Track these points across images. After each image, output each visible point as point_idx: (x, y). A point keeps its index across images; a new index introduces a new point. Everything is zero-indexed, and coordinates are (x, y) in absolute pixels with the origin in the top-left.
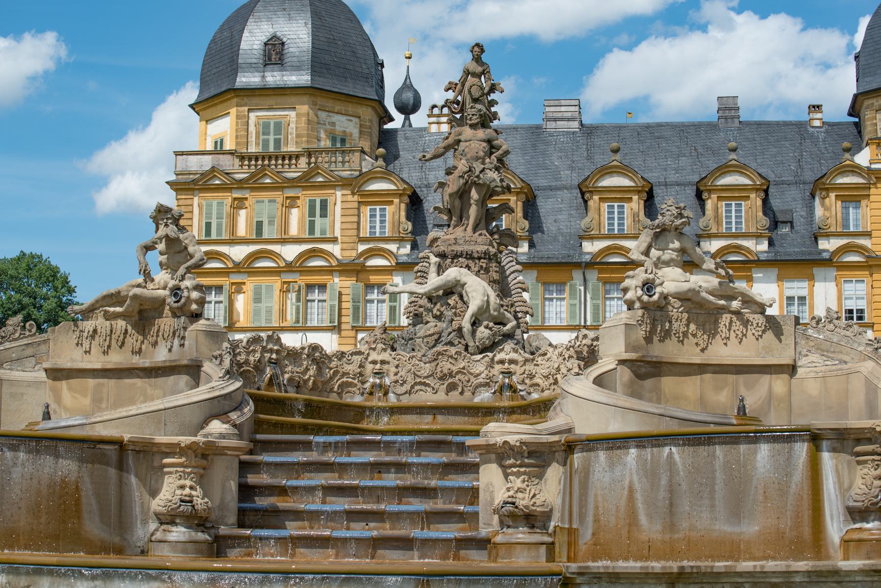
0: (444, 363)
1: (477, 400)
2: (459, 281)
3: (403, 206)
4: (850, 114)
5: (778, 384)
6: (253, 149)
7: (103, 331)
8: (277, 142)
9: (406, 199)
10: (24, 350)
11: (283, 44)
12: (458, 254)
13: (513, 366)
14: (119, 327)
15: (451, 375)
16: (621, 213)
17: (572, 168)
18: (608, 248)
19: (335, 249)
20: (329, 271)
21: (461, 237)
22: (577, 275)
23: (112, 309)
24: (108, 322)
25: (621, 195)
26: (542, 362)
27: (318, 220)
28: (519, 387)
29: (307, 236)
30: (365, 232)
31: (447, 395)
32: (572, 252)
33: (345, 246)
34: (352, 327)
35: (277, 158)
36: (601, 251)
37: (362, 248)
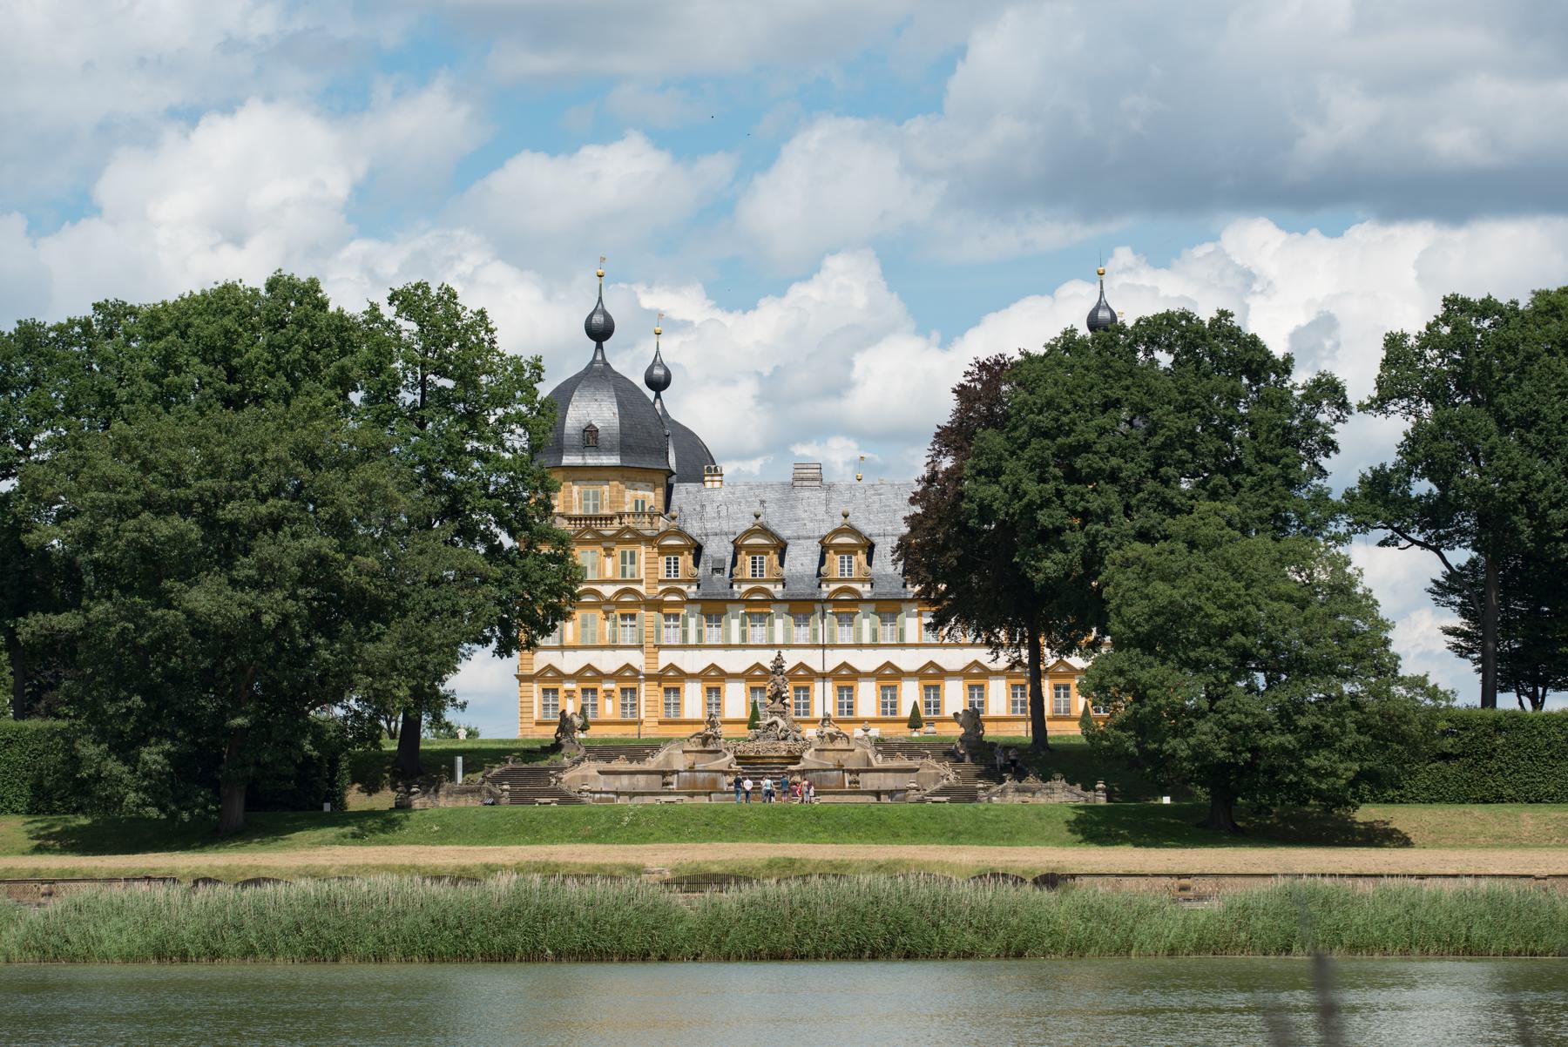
3: (691, 557)
5: (851, 753)
6: (576, 512)
8: (595, 506)
9: (693, 552)
11: (597, 431)
16: (850, 562)
17: (811, 521)
18: (840, 589)
19: (641, 589)
20: (637, 605)
22: (818, 607)
25: (848, 550)
27: (628, 566)
29: (620, 578)
30: (662, 575)
32: (814, 591)
33: (649, 586)
34: (655, 646)
35: (596, 519)
36: (835, 592)
37: (661, 588)
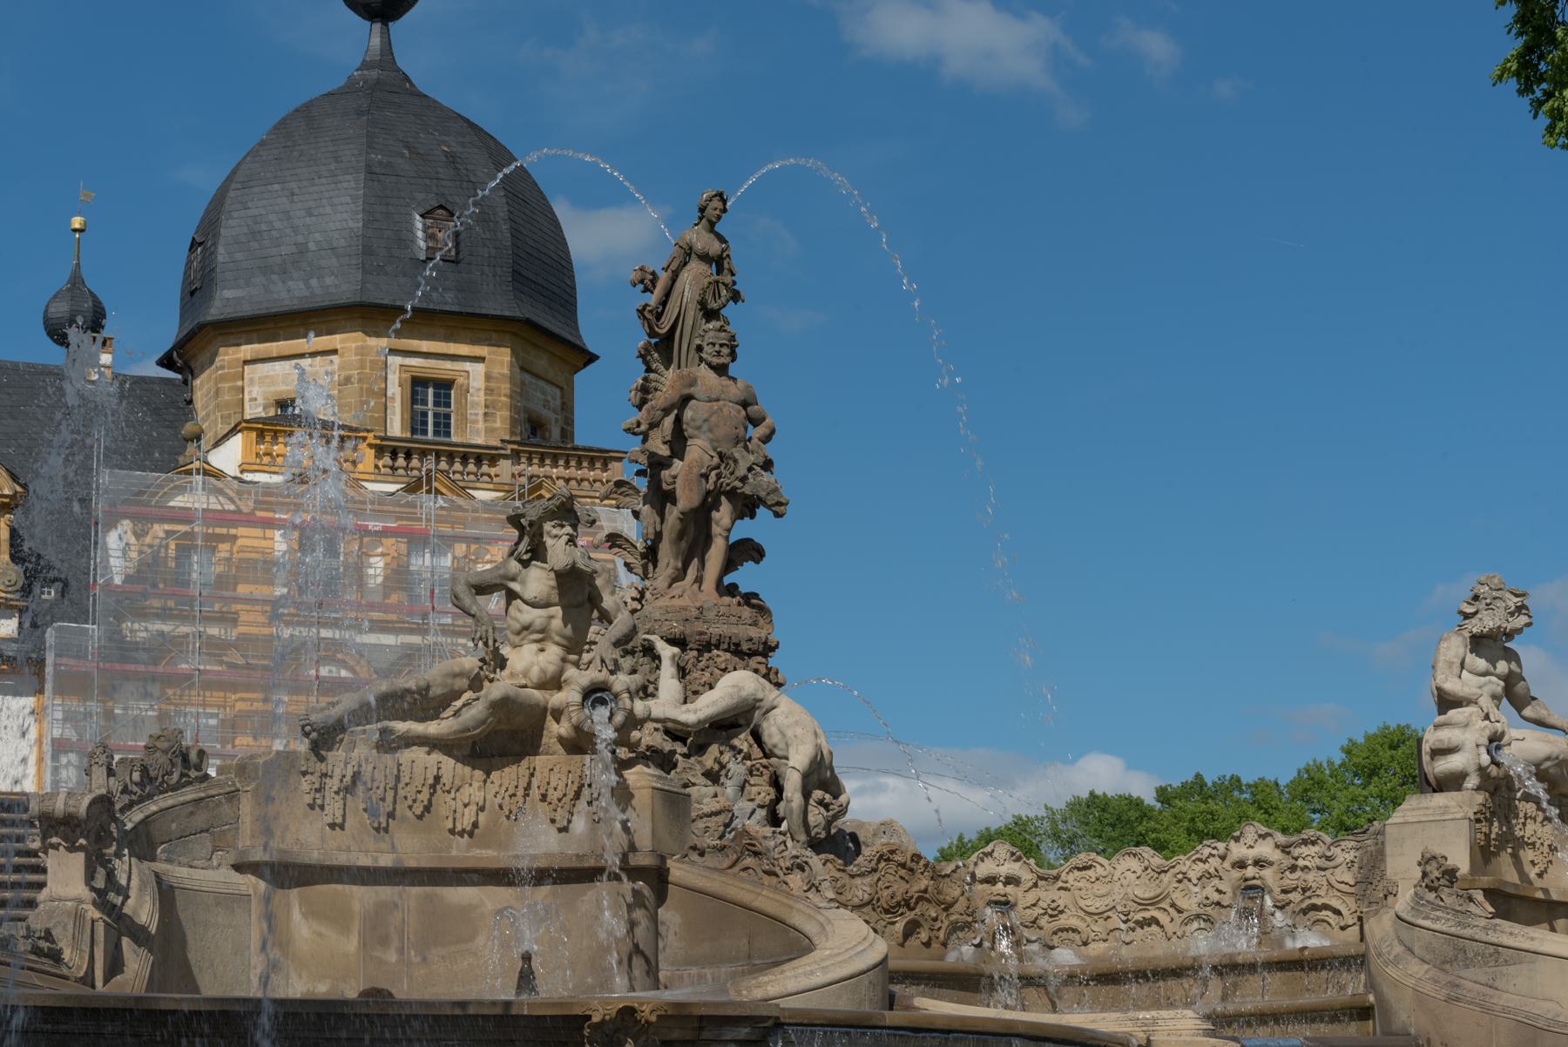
0: (891, 878)
1: (951, 957)
2: (761, 700)
4: (166, 362)
7: (379, 775)
10: (192, 813)
12: (714, 641)
13: (1010, 889)
14: (418, 770)
15: (908, 904)
21: (711, 604)
23: (401, 727)
24: (388, 759)
26: (1080, 885)
28: (1026, 933)
31: (902, 945)
